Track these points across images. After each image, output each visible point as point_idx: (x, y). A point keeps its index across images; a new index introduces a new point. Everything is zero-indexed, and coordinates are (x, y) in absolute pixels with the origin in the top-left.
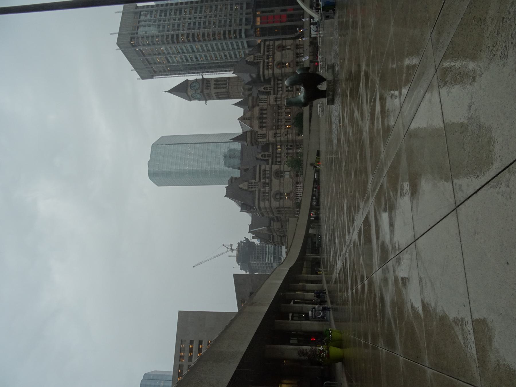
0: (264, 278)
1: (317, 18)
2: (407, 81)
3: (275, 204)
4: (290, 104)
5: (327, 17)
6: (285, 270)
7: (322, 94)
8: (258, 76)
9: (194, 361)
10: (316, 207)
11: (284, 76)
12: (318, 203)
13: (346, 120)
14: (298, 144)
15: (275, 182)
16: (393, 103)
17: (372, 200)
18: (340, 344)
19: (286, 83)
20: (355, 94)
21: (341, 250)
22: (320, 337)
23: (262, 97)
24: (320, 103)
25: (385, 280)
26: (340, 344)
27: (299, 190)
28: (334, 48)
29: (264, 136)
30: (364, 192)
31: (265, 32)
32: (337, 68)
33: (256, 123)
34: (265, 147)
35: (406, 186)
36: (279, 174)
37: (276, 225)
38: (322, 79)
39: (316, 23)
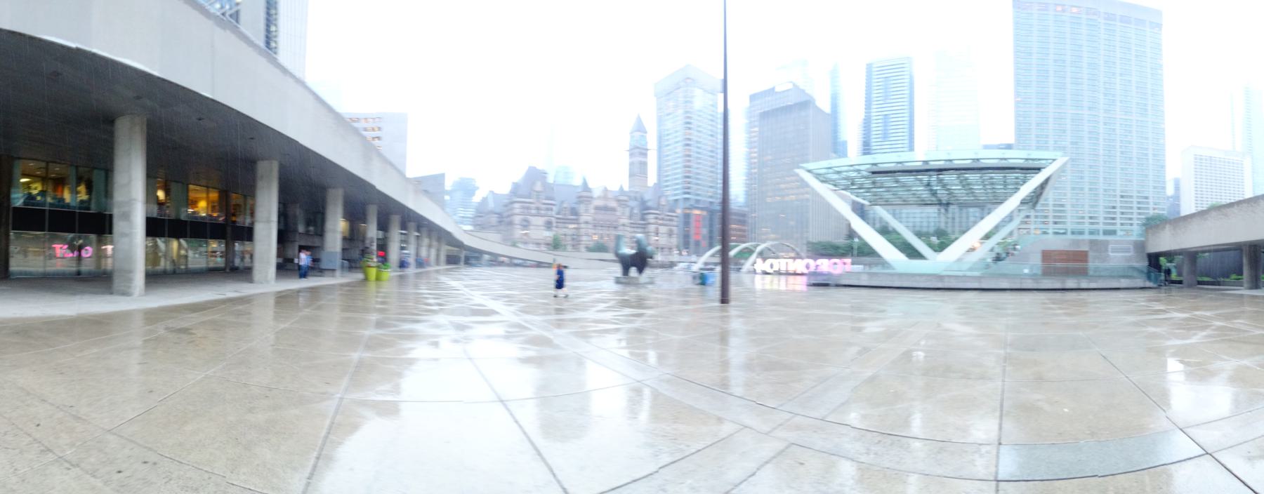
0: (442, 204)
1: (695, 268)
2: (631, 354)
3: (517, 219)
4: (618, 238)
5: (694, 278)
6: (448, 226)
7: (626, 271)
8: (648, 208)
9: (364, 133)
10: (513, 263)
11: (647, 233)
12: (517, 265)
13: (598, 296)
14: (576, 246)
15: (540, 221)
16: (612, 341)
17: (515, 319)
18: (378, 279)
19: (639, 236)
20: (625, 304)
21: (466, 286)
22: (384, 259)
23: (627, 211)
24: (617, 269)
25: (437, 326)
26: (378, 279)
27: (531, 247)
28: (665, 285)
29: (587, 211)
30: (524, 311)
31: (687, 217)
32: (650, 286)
33: (600, 203)
34: (574, 212)
35: (531, 353)
36: (549, 225)
37: (494, 219)
38: (640, 270)
39: (689, 267)
